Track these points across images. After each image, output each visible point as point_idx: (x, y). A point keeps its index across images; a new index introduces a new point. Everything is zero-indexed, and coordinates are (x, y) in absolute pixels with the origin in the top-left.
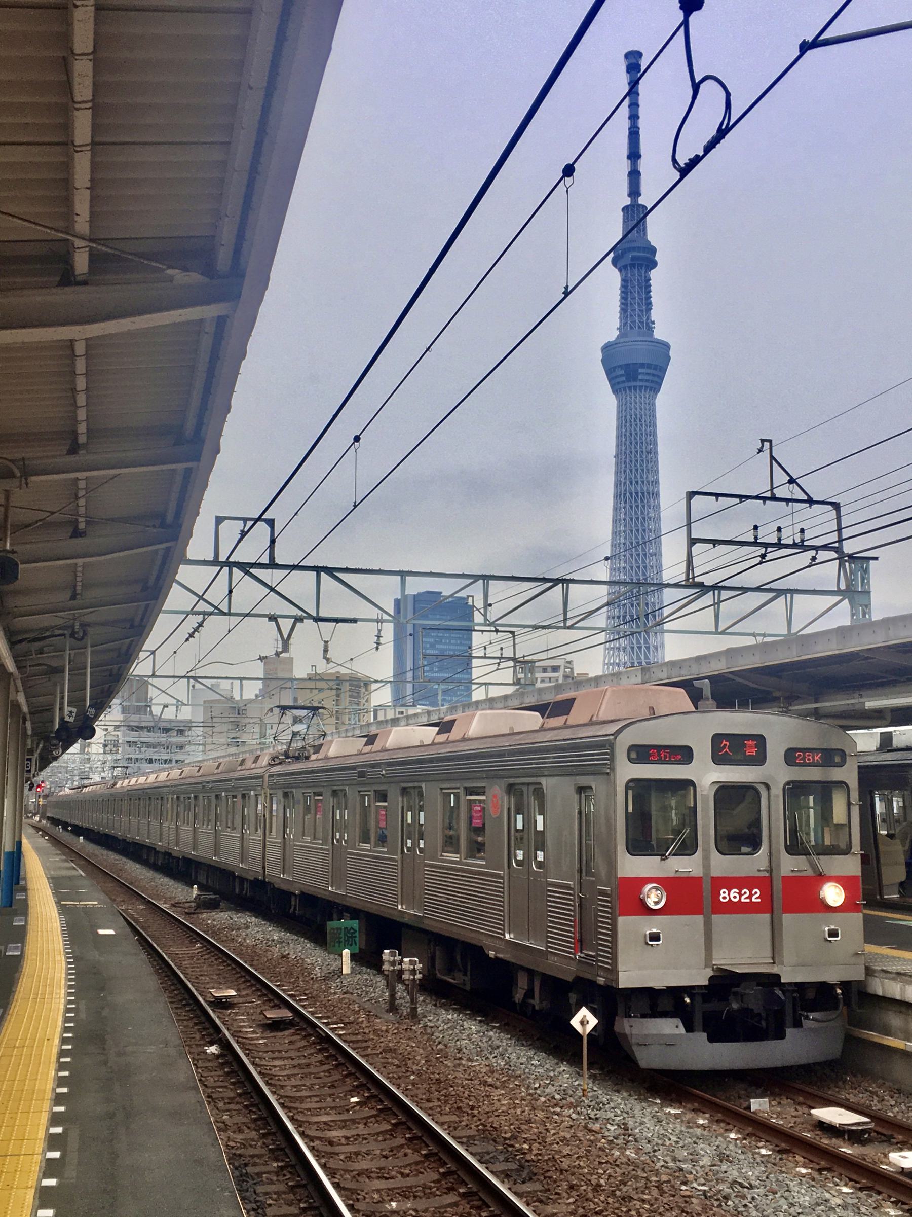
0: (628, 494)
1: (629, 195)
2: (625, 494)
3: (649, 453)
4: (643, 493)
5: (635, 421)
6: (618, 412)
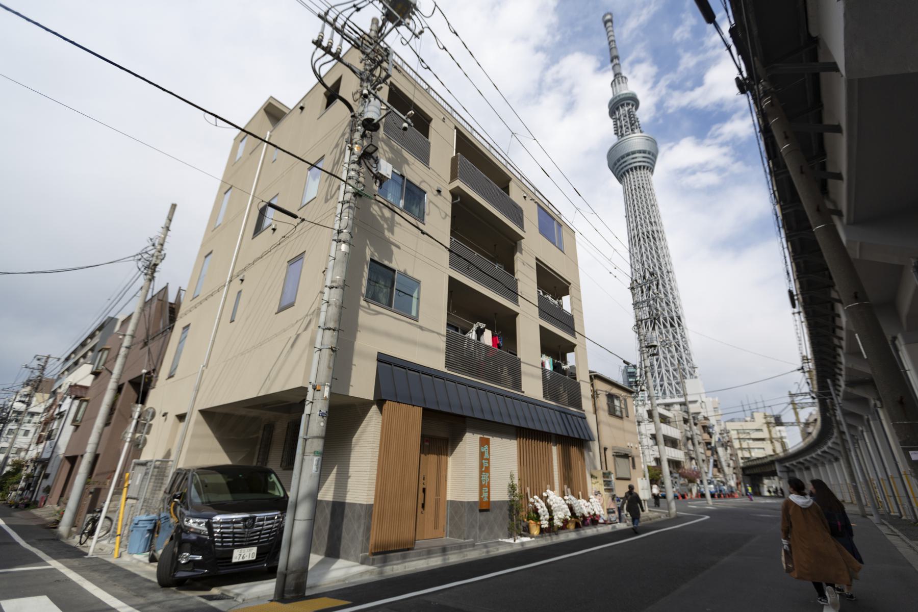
4: (653, 232)
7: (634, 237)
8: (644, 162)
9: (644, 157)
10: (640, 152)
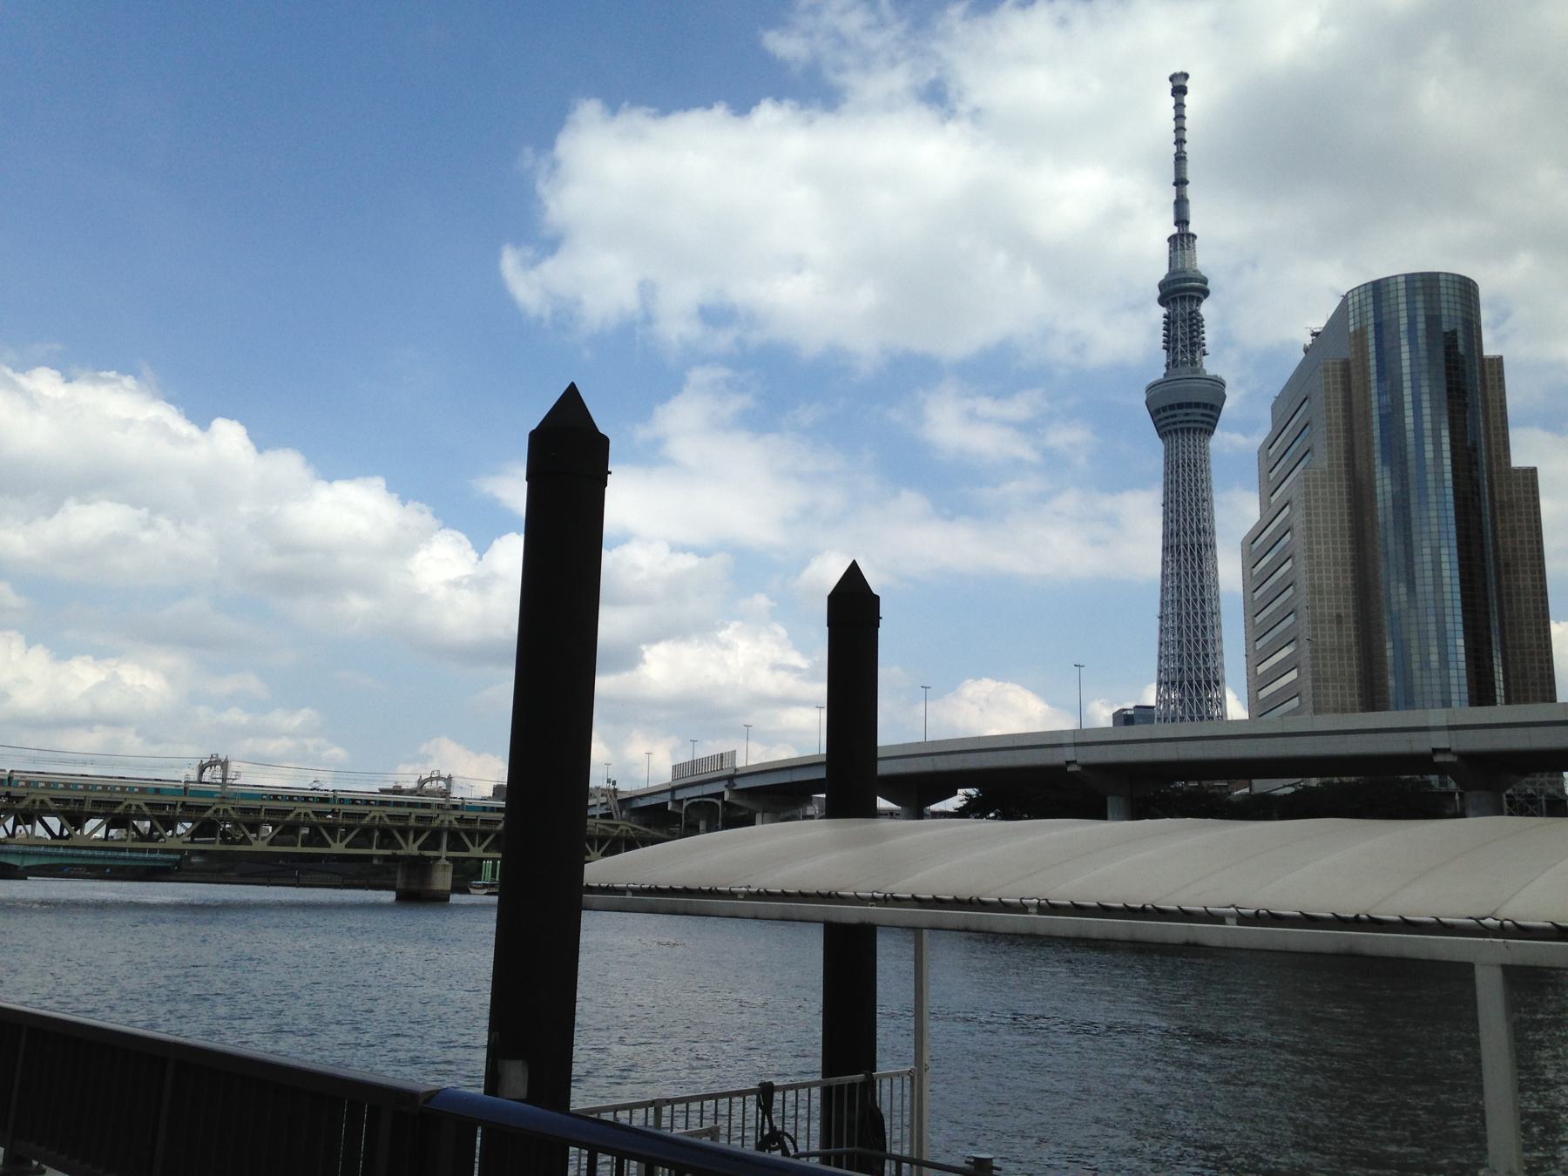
0: (1182, 546)
1: (1177, 224)
2: (1178, 546)
3: (1204, 500)
4: (1200, 545)
5: (1189, 465)
6: (1166, 457)
7: (1172, 547)
8: (1202, 422)
9: (1203, 415)
10: (1197, 405)
